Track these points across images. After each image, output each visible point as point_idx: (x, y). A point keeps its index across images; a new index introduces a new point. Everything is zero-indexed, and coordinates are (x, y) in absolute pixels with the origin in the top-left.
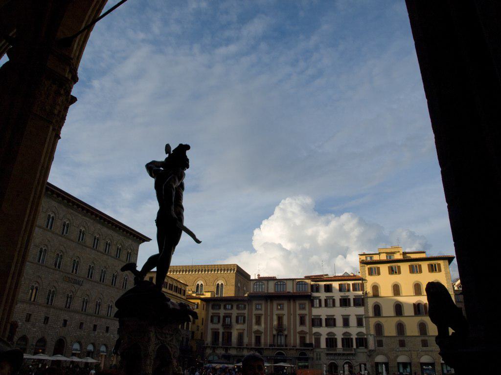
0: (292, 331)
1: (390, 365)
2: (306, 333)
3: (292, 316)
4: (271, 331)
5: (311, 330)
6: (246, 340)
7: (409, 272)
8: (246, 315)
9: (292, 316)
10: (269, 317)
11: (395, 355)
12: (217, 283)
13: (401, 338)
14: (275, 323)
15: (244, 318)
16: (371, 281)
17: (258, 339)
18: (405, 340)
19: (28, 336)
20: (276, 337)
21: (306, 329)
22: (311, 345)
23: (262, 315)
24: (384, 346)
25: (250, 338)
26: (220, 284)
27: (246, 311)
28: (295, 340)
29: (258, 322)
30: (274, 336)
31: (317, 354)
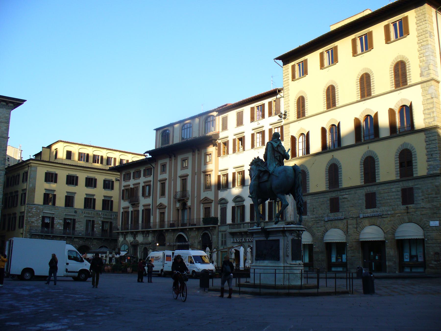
1: (316, 249)
5: (216, 195)
7: (351, 54)
9: (196, 176)
11: (323, 229)
13: (334, 195)
14: (179, 189)
16: (292, 91)
18: (340, 197)
20: (180, 211)
22: (215, 220)
23: (166, 180)
24: (308, 213)
28: (198, 214)
30: (178, 210)
31: (222, 234)
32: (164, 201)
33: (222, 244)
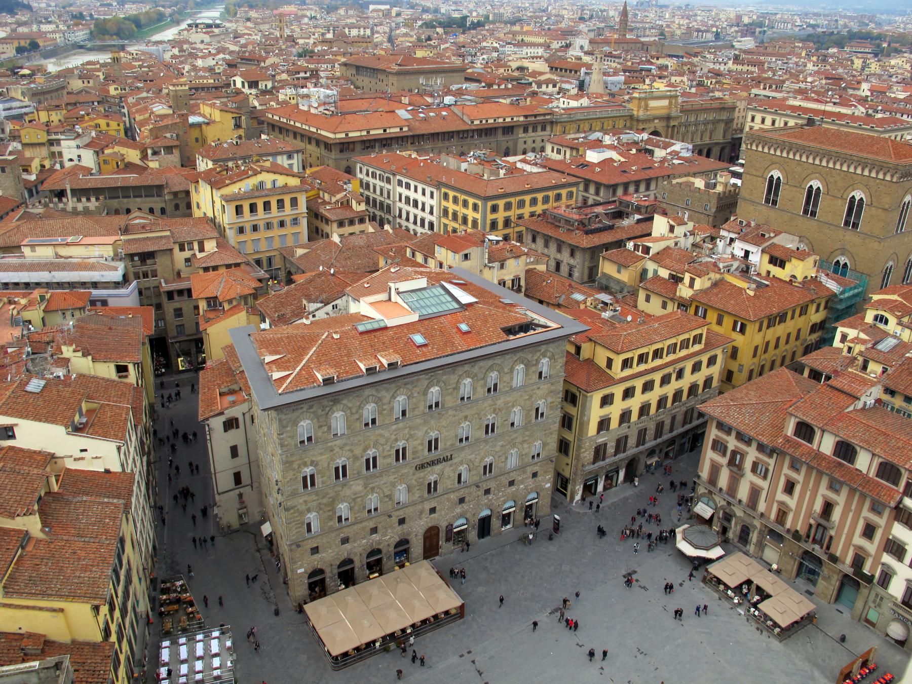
0: (844, 537)
2: (869, 555)
3: (851, 514)
4: (809, 513)
6: (762, 507)
8: (771, 468)
9: (851, 514)
10: (808, 493)
12: (850, 196)
14: (818, 506)
15: (767, 470)
17: (782, 514)
19: (381, 547)
21: (871, 547)
25: (769, 508)
26: (857, 198)
27: (772, 462)
29: (789, 488)
30: (811, 526)
32: (792, 502)
33: (874, 602)
